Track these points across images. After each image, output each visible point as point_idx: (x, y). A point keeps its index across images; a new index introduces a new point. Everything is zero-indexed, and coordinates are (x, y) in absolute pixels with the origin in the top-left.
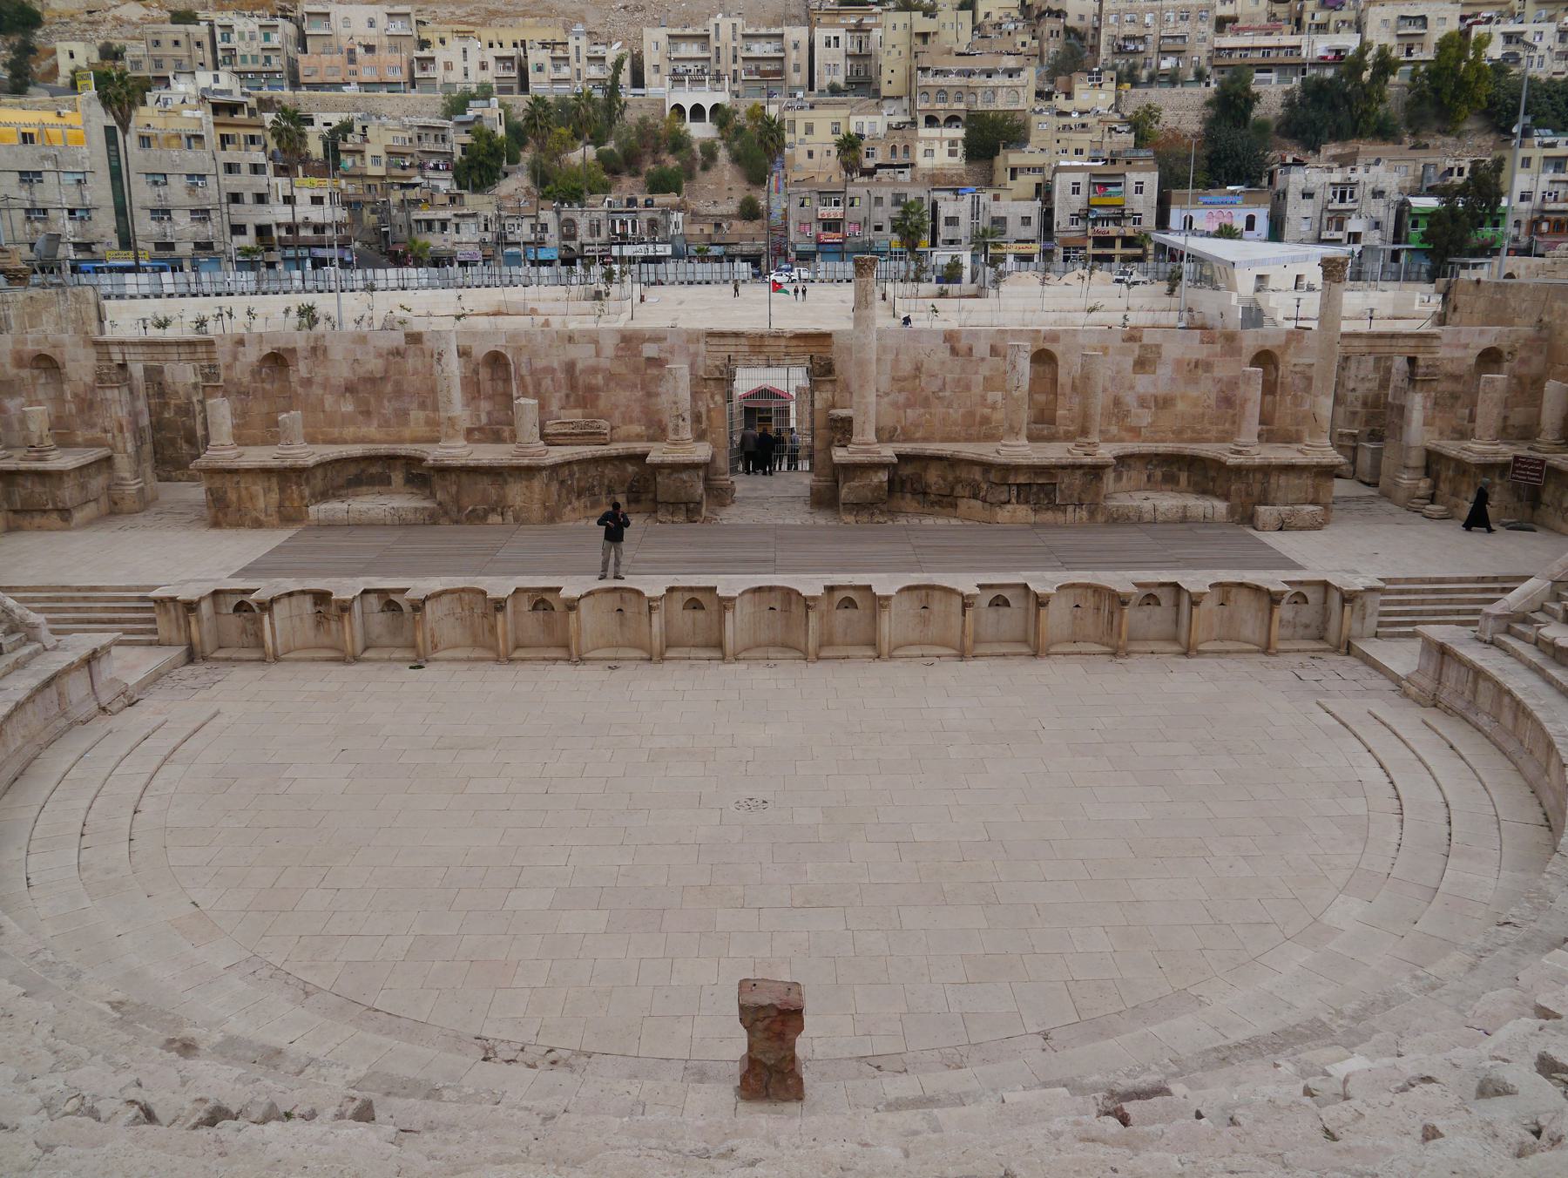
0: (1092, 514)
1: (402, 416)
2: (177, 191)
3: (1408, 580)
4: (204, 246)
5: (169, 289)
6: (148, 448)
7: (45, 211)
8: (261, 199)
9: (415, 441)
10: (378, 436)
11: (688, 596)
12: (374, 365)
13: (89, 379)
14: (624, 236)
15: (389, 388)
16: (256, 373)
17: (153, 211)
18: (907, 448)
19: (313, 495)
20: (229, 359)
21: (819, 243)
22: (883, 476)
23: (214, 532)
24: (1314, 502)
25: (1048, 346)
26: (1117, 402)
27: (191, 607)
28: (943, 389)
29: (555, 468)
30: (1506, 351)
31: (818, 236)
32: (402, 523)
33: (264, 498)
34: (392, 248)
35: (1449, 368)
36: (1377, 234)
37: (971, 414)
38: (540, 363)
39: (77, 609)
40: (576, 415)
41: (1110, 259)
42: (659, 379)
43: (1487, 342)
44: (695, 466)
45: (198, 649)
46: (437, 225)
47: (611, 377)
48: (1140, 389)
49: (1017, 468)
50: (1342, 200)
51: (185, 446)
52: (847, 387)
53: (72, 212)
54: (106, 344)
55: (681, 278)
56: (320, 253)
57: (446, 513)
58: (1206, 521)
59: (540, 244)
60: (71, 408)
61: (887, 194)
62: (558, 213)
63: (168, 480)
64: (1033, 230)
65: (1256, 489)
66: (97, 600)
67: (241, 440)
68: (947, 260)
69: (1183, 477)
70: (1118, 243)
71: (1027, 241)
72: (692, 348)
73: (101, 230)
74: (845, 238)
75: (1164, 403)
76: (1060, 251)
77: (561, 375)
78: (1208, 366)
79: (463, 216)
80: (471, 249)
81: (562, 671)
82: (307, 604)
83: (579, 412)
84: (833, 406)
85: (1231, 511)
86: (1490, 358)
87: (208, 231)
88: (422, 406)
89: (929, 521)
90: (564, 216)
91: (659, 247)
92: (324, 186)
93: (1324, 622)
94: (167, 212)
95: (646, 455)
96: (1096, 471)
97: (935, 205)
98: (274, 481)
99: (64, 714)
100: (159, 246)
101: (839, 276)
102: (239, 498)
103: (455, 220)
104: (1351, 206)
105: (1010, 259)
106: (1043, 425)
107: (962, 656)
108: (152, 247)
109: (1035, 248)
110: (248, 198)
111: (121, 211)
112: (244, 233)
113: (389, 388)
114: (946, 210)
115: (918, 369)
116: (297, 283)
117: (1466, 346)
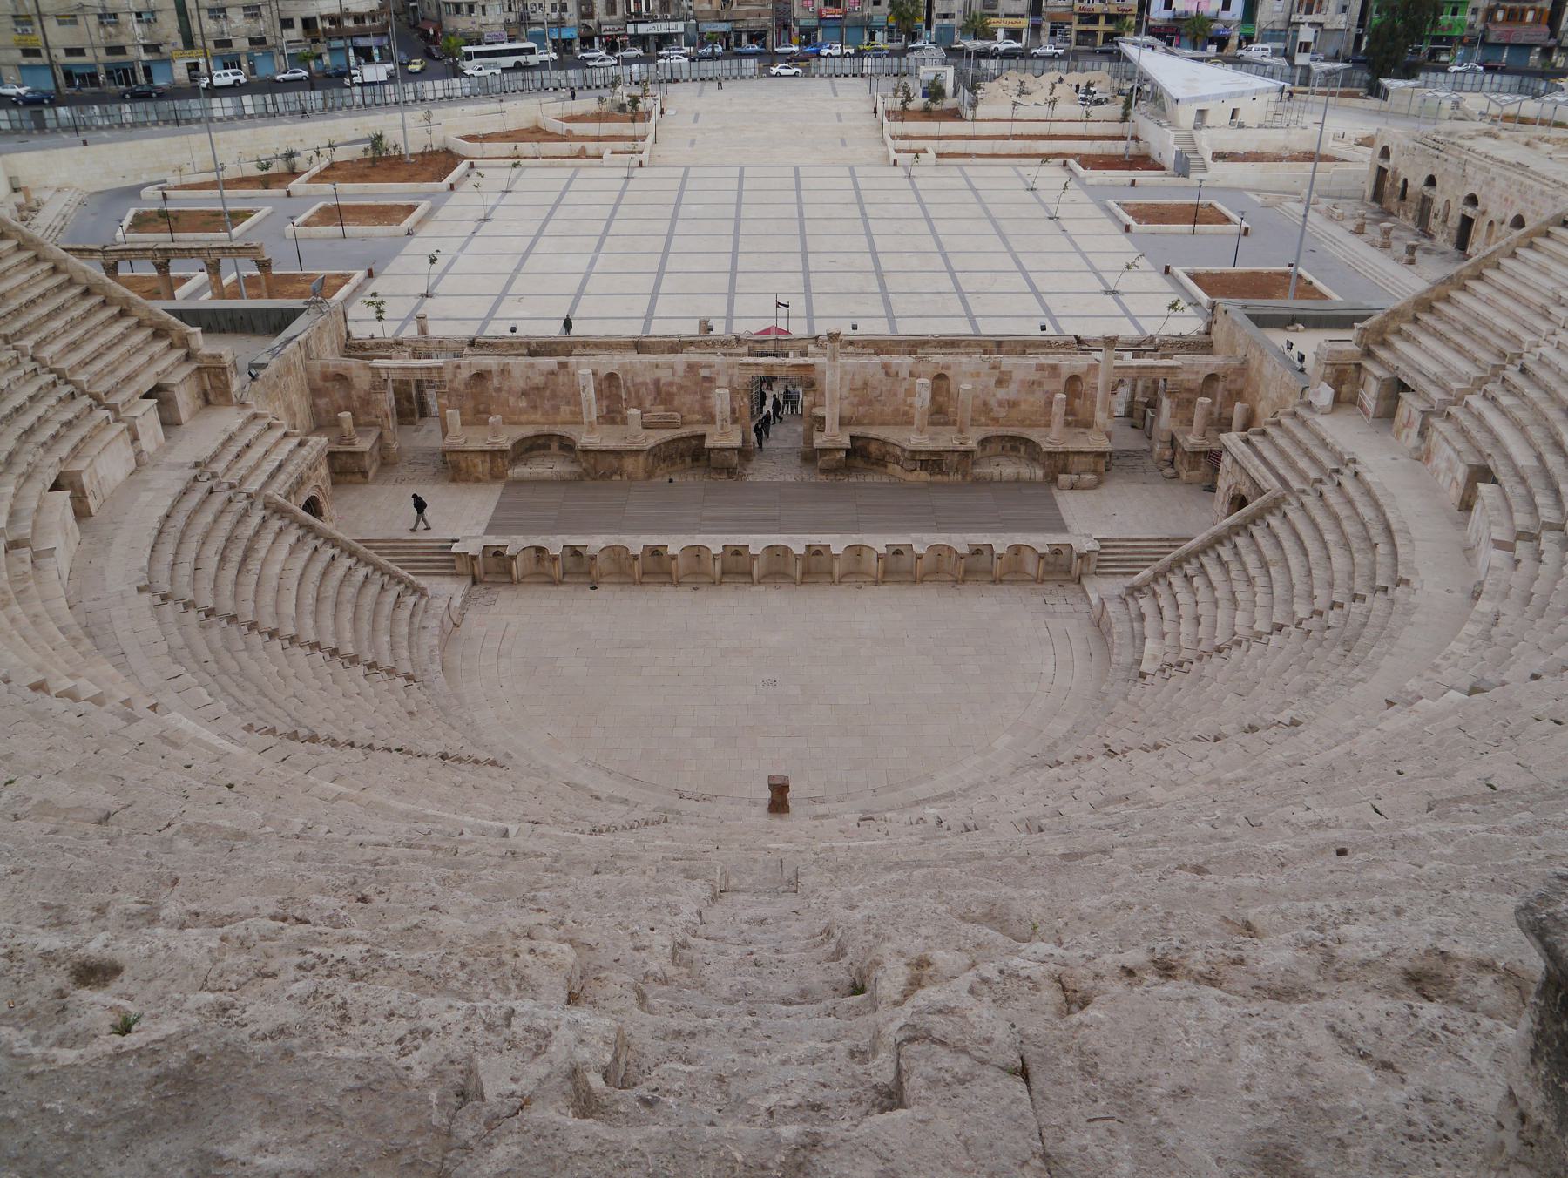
0: (964, 477)
1: (556, 409)
5: (249, 110)
7: (115, 16)
9: (564, 423)
10: (542, 420)
12: (539, 380)
13: (367, 388)
14: (638, 14)
15: (548, 393)
16: (467, 384)
17: (210, 10)
18: (858, 431)
21: (821, 18)
22: (843, 454)
23: (453, 486)
24: (1094, 472)
26: (985, 404)
29: (651, 450)
31: (820, 11)
32: (562, 481)
33: (482, 466)
34: (422, 25)
35: (1186, 385)
36: (1343, 18)
37: (897, 410)
38: (639, 380)
40: (659, 411)
41: (1094, 33)
42: (710, 389)
43: (1209, 371)
46: (465, 8)
47: (681, 387)
52: (823, 394)
55: (694, 75)
56: (362, 42)
58: (1031, 483)
59: (561, 23)
65: (1061, 463)
68: (932, 77)
69: (1023, 449)
70: (1102, 20)
71: (1017, 16)
73: (165, 32)
74: (845, 13)
75: (1013, 404)
76: (1047, 25)
77: (651, 387)
78: (1040, 384)
80: (497, 29)
81: (668, 592)
82: (533, 552)
84: (815, 405)
85: (1046, 475)
86: (1212, 378)
88: (568, 403)
89: (869, 479)
91: (672, 25)
93: (1063, 569)
94: (223, 10)
95: (703, 436)
96: (967, 454)
98: (488, 458)
100: (219, 44)
101: (838, 71)
105: (1000, 33)
106: (939, 413)
107: (876, 583)
109: (1024, 23)
112: (292, 26)
113: (548, 393)
115: (866, 384)
116: (358, 99)
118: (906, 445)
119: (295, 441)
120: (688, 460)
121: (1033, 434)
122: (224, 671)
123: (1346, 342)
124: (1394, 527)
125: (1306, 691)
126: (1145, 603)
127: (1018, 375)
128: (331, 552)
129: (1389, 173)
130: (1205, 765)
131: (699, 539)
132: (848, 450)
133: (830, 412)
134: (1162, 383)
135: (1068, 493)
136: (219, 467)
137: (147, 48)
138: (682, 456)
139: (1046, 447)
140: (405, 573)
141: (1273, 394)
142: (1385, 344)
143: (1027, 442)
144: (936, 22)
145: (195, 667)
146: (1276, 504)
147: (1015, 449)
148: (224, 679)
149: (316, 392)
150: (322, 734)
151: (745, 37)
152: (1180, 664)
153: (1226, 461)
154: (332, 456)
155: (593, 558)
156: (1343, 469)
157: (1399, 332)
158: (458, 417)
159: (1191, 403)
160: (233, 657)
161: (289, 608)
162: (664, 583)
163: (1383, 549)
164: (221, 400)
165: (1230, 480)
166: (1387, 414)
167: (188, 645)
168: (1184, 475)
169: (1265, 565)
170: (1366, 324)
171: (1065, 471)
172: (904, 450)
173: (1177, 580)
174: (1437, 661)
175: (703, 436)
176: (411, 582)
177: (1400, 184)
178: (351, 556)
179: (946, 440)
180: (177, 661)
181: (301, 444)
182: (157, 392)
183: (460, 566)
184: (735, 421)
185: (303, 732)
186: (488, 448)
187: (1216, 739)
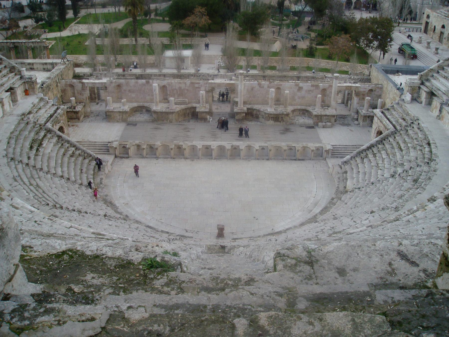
18: (249, 106)
22: (244, 114)
23: (109, 124)
29: (178, 112)
32: (146, 122)
33: (118, 117)
39: (93, 147)
42: (199, 91)
43: (370, 88)
49: (271, 114)
54: (84, 83)
69: (306, 114)
75: (303, 97)
82: (136, 147)
86: (371, 90)
96: (287, 115)
98: (121, 114)
106: (278, 102)
118: (266, 111)
119: (56, 107)
120: (190, 116)
121: (310, 109)
122: (31, 184)
123: (415, 78)
124: (431, 142)
125: (401, 197)
126: (347, 167)
127: (305, 88)
128: (68, 145)
129: (430, 24)
130: (367, 221)
131: (194, 143)
132: (246, 113)
133: (239, 99)
134: (354, 92)
135: (322, 129)
136: (31, 116)
139: (315, 113)
140: (92, 153)
141: (391, 96)
142: (428, 80)
143: (307, 111)
145: (22, 183)
146: (393, 134)
148: (32, 188)
150: (64, 206)
152: (359, 188)
153: (375, 119)
155: (157, 149)
156: (415, 122)
157: (433, 76)
158: (111, 100)
159: (364, 99)
160: (35, 180)
161: (53, 164)
162: (181, 158)
163: (427, 149)
164: (31, 93)
166: (429, 103)
167: (19, 176)
168: (361, 123)
169: (388, 154)
170: (422, 73)
172: (265, 113)
173: (358, 160)
174: (445, 187)
175: (196, 108)
177: (433, 27)
178: (74, 147)
179: (280, 110)
180: (16, 180)
181: (58, 109)
182: (11, 90)
184: (207, 102)
185: (58, 206)
186: (122, 110)
187: (371, 213)
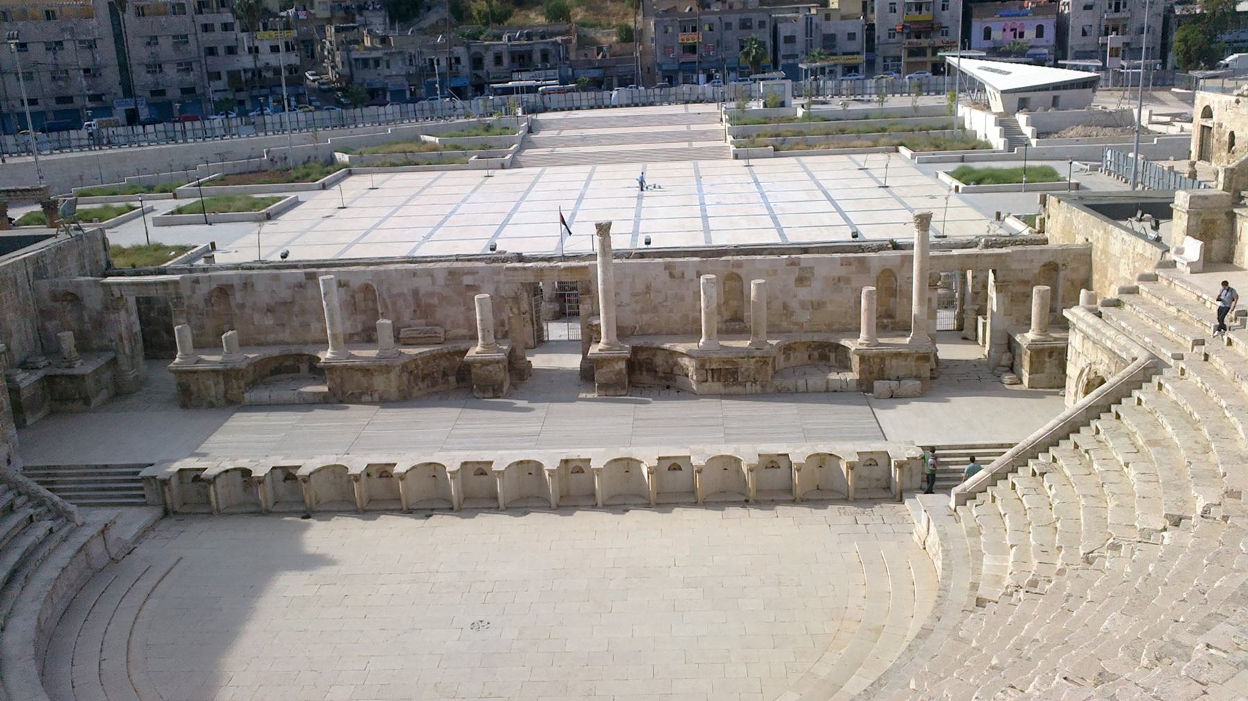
1: (306, 326)
2: (165, 46)
3: (950, 447)
4: (188, 91)
6: (140, 345)
8: (231, 50)
10: (290, 340)
11: (477, 466)
12: (285, 294)
13: (99, 307)
16: (208, 301)
17: (148, 66)
18: (639, 342)
19: (247, 385)
20: (189, 293)
22: (622, 365)
24: (917, 377)
25: (735, 270)
26: (785, 306)
27: (165, 482)
28: (666, 300)
30: (1060, 263)
33: (215, 389)
37: (686, 316)
38: (395, 291)
39: (96, 482)
44: (498, 362)
45: (170, 507)
47: (443, 298)
48: (801, 297)
50: (1117, 10)
51: (165, 336)
53: (86, 71)
54: (109, 285)
57: (334, 395)
59: (456, 75)
60: (88, 326)
61: (735, 19)
62: (468, 47)
63: (156, 358)
64: (859, 43)
66: (107, 474)
67: (199, 345)
69: (832, 356)
71: (852, 54)
72: (496, 278)
75: (818, 306)
77: (410, 298)
78: (847, 280)
79: (392, 54)
82: (239, 474)
83: (423, 321)
87: (191, 78)
90: (473, 50)
92: (280, 38)
97: (775, 28)
98: (221, 379)
99: (89, 566)
100: (153, 93)
102: (199, 389)
103: (386, 58)
104: (1124, 15)
108: (148, 94)
109: (861, 59)
110: (221, 51)
111: (124, 67)
114: (784, 30)
115: (648, 288)
117: (1032, 261)
120: (452, 379)
127: (821, 272)
129: (1214, 130)
137: (94, 98)
138: (445, 374)
144: (782, 62)
147: (824, 357)
149: (45, 314)
151: (615, 81)
152: (1034, 584)
154: (49, 380)
165: (1082, 363)
171: (881, 377)
176: (55, 504)
177: (1226, 138)
183: (150, 496)
